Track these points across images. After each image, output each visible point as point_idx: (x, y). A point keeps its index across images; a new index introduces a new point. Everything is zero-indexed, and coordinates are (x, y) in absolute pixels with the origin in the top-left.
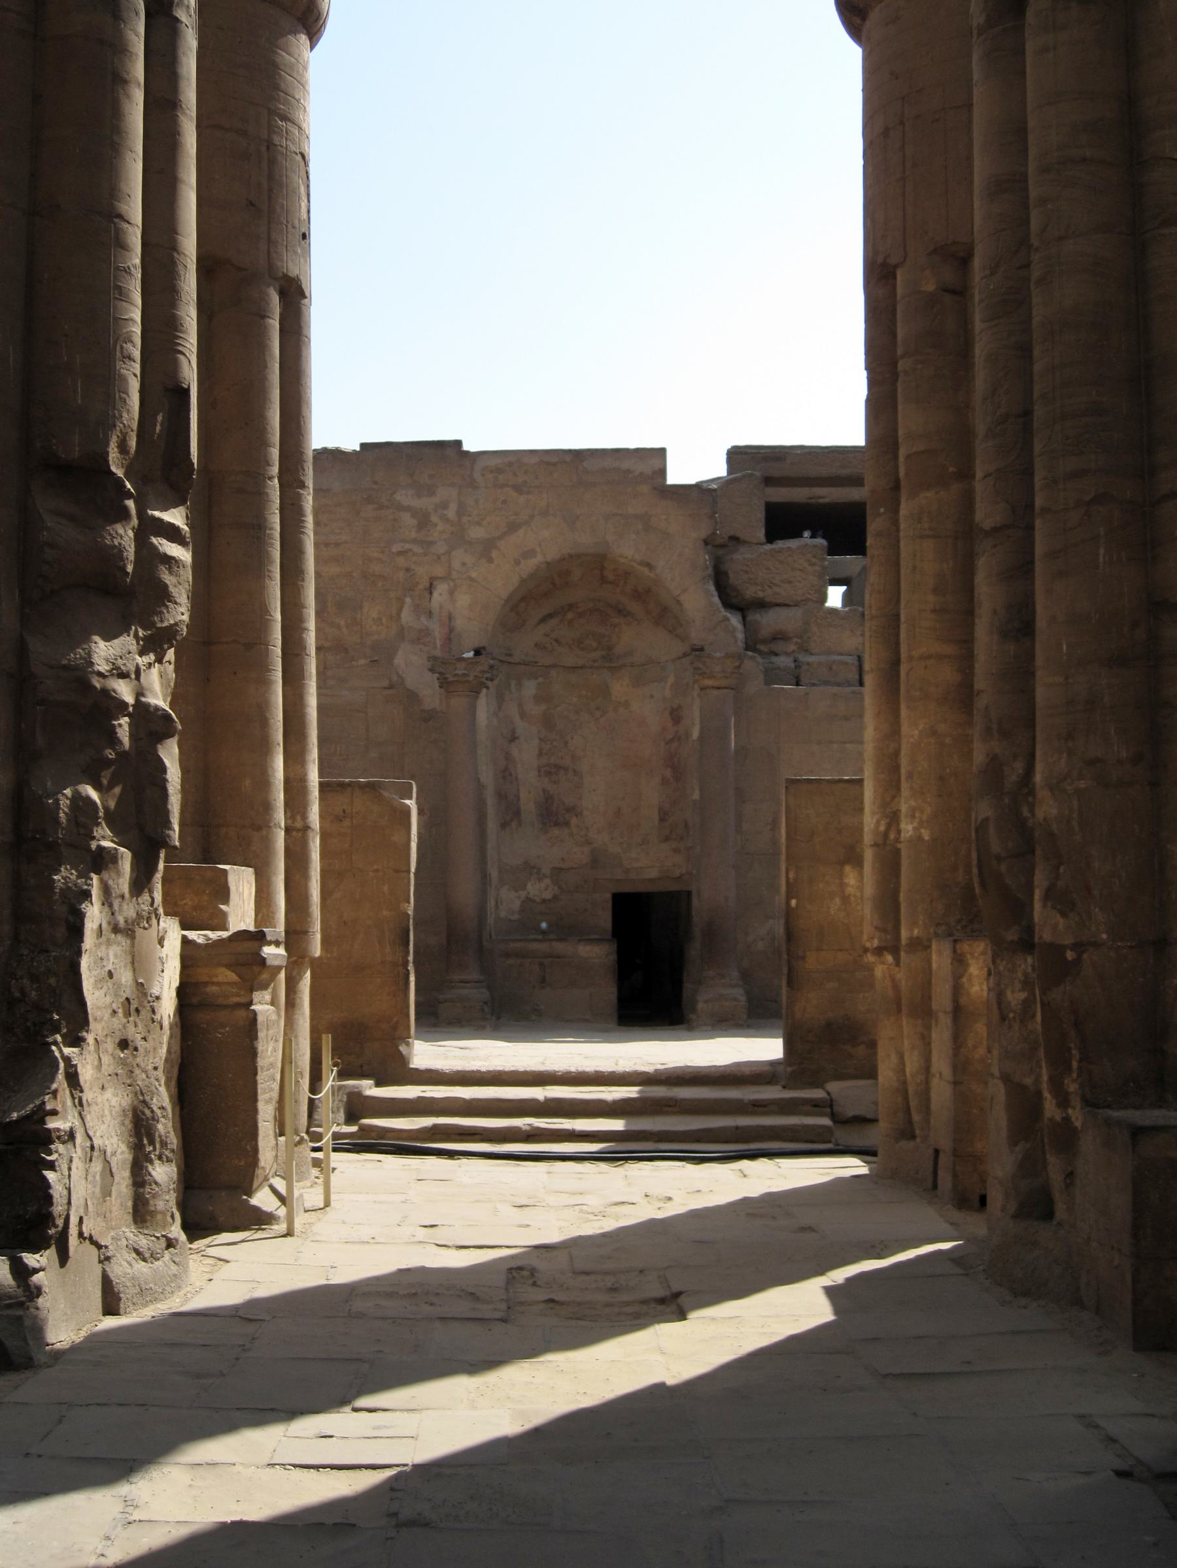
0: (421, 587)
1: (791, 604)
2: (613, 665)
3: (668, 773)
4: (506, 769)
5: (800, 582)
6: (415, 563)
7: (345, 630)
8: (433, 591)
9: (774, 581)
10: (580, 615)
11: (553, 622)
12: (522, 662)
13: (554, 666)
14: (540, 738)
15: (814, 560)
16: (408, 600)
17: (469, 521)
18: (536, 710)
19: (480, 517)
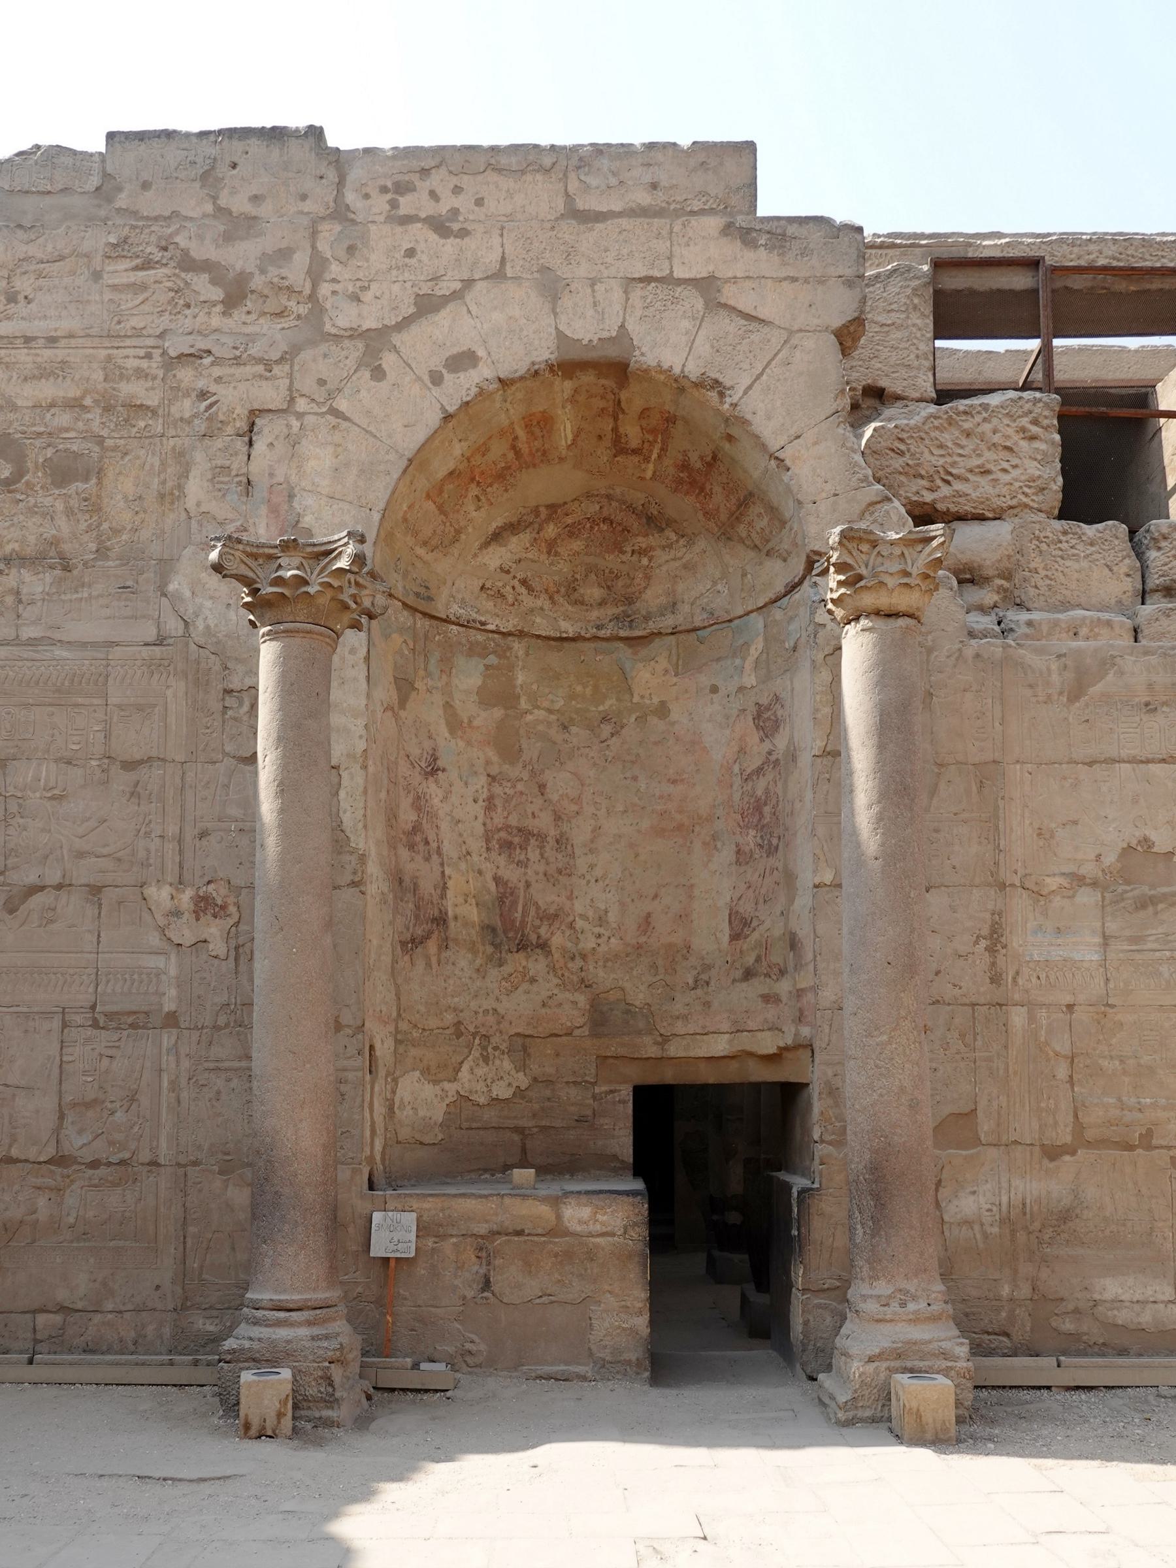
0: (230, 430)
1: (990, 515)
3: (750, 839)
4: (416, 829)
5: (1004, 470)
6: (218, 380)
7: (62, 521)
8: (254, 439)
9: (954, 471)
10: (572, 532)
11: (517, 544)
12: (453, 619)
13: (521, 634)
14: (489, 775)
15: (1034, 429)
16: (199, 456)
17: (334, 293)
18: (487, 718)
19: (359, 284)
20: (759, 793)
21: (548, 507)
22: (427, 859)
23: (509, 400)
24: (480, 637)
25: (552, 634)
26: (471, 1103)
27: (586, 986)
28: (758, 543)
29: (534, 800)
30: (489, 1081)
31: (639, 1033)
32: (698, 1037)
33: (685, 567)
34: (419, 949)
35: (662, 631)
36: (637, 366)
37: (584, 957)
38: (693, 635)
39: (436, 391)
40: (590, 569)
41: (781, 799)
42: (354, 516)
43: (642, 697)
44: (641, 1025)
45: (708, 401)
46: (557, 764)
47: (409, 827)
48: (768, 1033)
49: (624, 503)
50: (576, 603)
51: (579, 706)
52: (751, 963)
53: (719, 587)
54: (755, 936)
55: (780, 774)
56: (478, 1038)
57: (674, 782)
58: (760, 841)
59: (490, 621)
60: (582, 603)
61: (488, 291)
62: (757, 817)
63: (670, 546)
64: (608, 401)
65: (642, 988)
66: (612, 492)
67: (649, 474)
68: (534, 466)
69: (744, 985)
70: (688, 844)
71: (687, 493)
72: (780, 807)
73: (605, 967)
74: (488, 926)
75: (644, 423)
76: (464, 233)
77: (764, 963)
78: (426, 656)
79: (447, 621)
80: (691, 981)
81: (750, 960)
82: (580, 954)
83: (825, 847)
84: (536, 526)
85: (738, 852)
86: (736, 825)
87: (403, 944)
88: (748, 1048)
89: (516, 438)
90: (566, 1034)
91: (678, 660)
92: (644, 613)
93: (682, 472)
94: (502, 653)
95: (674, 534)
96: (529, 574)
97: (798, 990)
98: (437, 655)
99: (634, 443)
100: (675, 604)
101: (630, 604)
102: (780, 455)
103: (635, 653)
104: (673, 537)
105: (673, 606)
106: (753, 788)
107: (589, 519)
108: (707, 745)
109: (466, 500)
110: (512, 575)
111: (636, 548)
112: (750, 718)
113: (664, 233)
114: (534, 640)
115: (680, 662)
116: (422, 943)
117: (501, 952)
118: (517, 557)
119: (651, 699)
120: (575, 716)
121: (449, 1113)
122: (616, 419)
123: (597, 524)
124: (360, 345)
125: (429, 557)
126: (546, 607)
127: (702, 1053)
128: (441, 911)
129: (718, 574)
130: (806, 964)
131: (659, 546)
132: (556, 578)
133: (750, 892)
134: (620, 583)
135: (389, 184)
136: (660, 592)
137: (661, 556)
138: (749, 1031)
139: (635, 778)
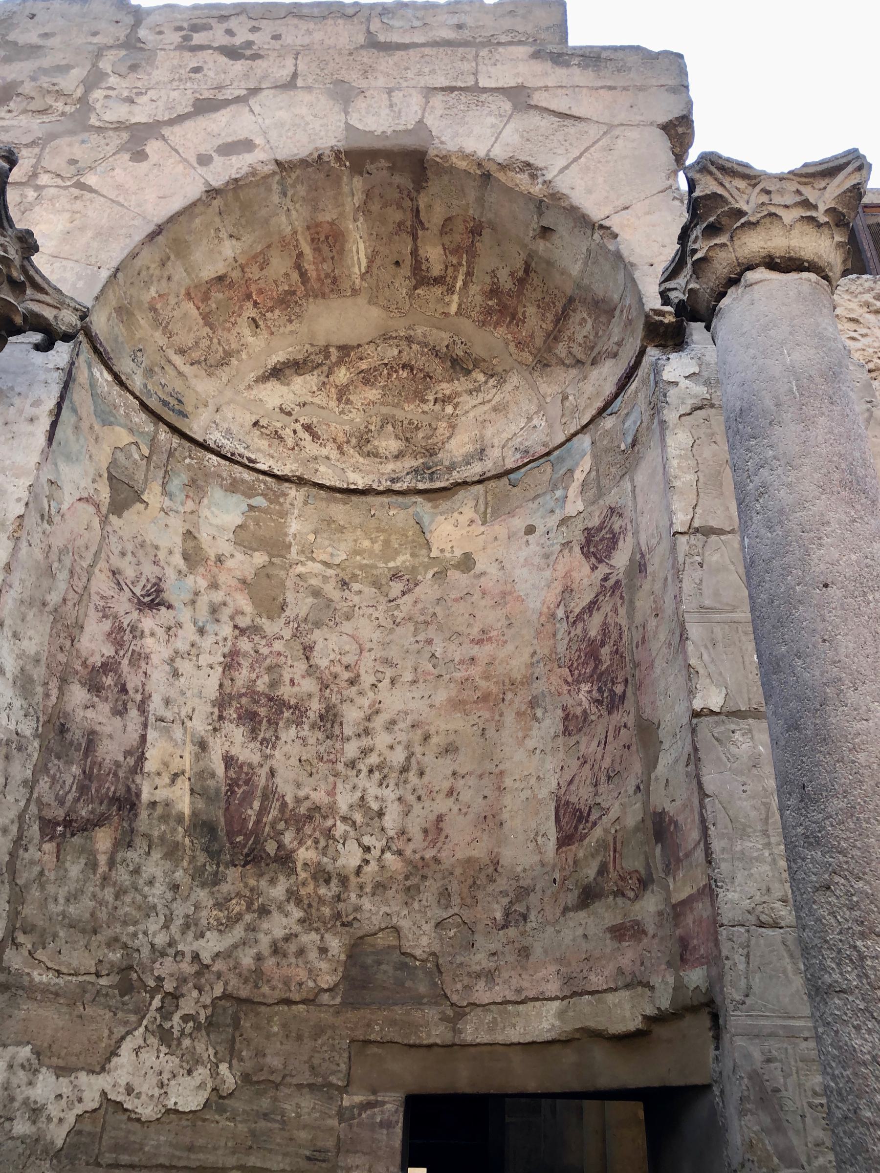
2: (438, 485)
4: (108, 667)
10: (367, 378)
12: (212, 445)
13: (300, 481)
14: (236, 627)
19: (134, 91)
20: (593, 633)
21: (340, 348)
22: (120, 711)
23: (290, 194)
24: (247, 476)
25: (339, 484)
26: (125, 1117)
27: (343, 925)
28: (580, 356)
29: (296, 664)
30: (166, 1076)
31: (418, 1001)
32: (510, 1007)
33: (495, 409)
34: (77, 840)
35: (468, 480)
36: (435, 152)
37: (344, 881)
38: (505, 480)
39: (201, 170)
40: (386, 421)
41: (625, 629)
42: (77, 273)
43: (442, 551)
44: (422, 988)
45: (517, 185)
46: (331, 623)
47: (97, 660)
48: (624, 994)
49: (426, 346)
50: (368, 455)
51: (365, 562)
52: (591, 878)
53: (536, 421)
54: (598, 832)
55: (622, 598)
56: (158, 997)
57: (479, 642)
58: (595, 694)
59: (263, 460)
60: (376, 455)
61: (274, 96)
62: (592, 665)
63: (478, 390)
64: (404, 211)
65: (428, 928)
66: (412, 333)
67: (454, 308)
68: (323, 296)
69: (582, 914)
70: (497, 718)
71: (497, 324)
72: (625, 639)
73: (373, 895)
74: (204, 823)
75: (446, 240)
76: (256, 57)
77: (613, 875)
78: (166, 472)
79: (203, 446)
80: (499, 915)
81: (590, 871)
82: (339, 874)
83: (706, 657)
84: (325, 368)
85: (566, 718)
86: (561, 682)
87: (48, 826)
88: (592, 1024)
89: (300, 255)
90: (303, 1002)
91: (486, 509)
92: (447, 463)
93: (491, 299)
94: (274, 498)
95: (482, 375)
96: (315, 420)
97: (674, 907)
98: (184, 478)
99: (436, 270)
100: (483, 450)
101: (431, 455)
102: (606, 223)
103: (436, 507)
104: (481, 378)
105: (481, 453)
106: (585, 630)
107: (386, 365)
108: (522, 594)
109: (239, 320)
110: (293, 418)
111: (440, 395)
112: (577, 549)
113: (470, 57)
114: (314, 491)
115: (489, 511)
116: (85, 830)
117: (218, 865)
118: (302, 400)
119: (453, 551)
120: (358, 572)
121: (79, 1133)
122: (415, 238)
123: (396, 371)
124: (125, 136)
125: (186, 369)
126: (331, 456)
127: (514, 1035)
128: (129, 789)
129: (533, 408)
130: (687, 855)
131: (466, 391)
132: (347, 428)
133: (586, 771)
134: (421, 435)
135: (185, 25)
136: (466, 440)
137: (467, 401)
138: (592, 993)
139: (429, 642)
